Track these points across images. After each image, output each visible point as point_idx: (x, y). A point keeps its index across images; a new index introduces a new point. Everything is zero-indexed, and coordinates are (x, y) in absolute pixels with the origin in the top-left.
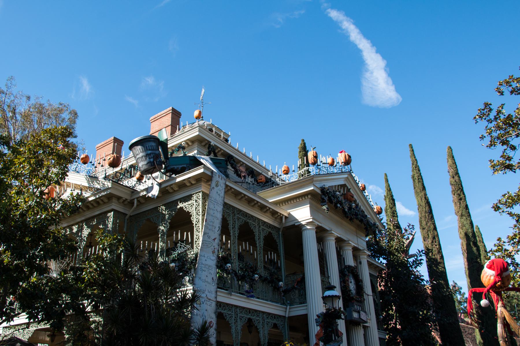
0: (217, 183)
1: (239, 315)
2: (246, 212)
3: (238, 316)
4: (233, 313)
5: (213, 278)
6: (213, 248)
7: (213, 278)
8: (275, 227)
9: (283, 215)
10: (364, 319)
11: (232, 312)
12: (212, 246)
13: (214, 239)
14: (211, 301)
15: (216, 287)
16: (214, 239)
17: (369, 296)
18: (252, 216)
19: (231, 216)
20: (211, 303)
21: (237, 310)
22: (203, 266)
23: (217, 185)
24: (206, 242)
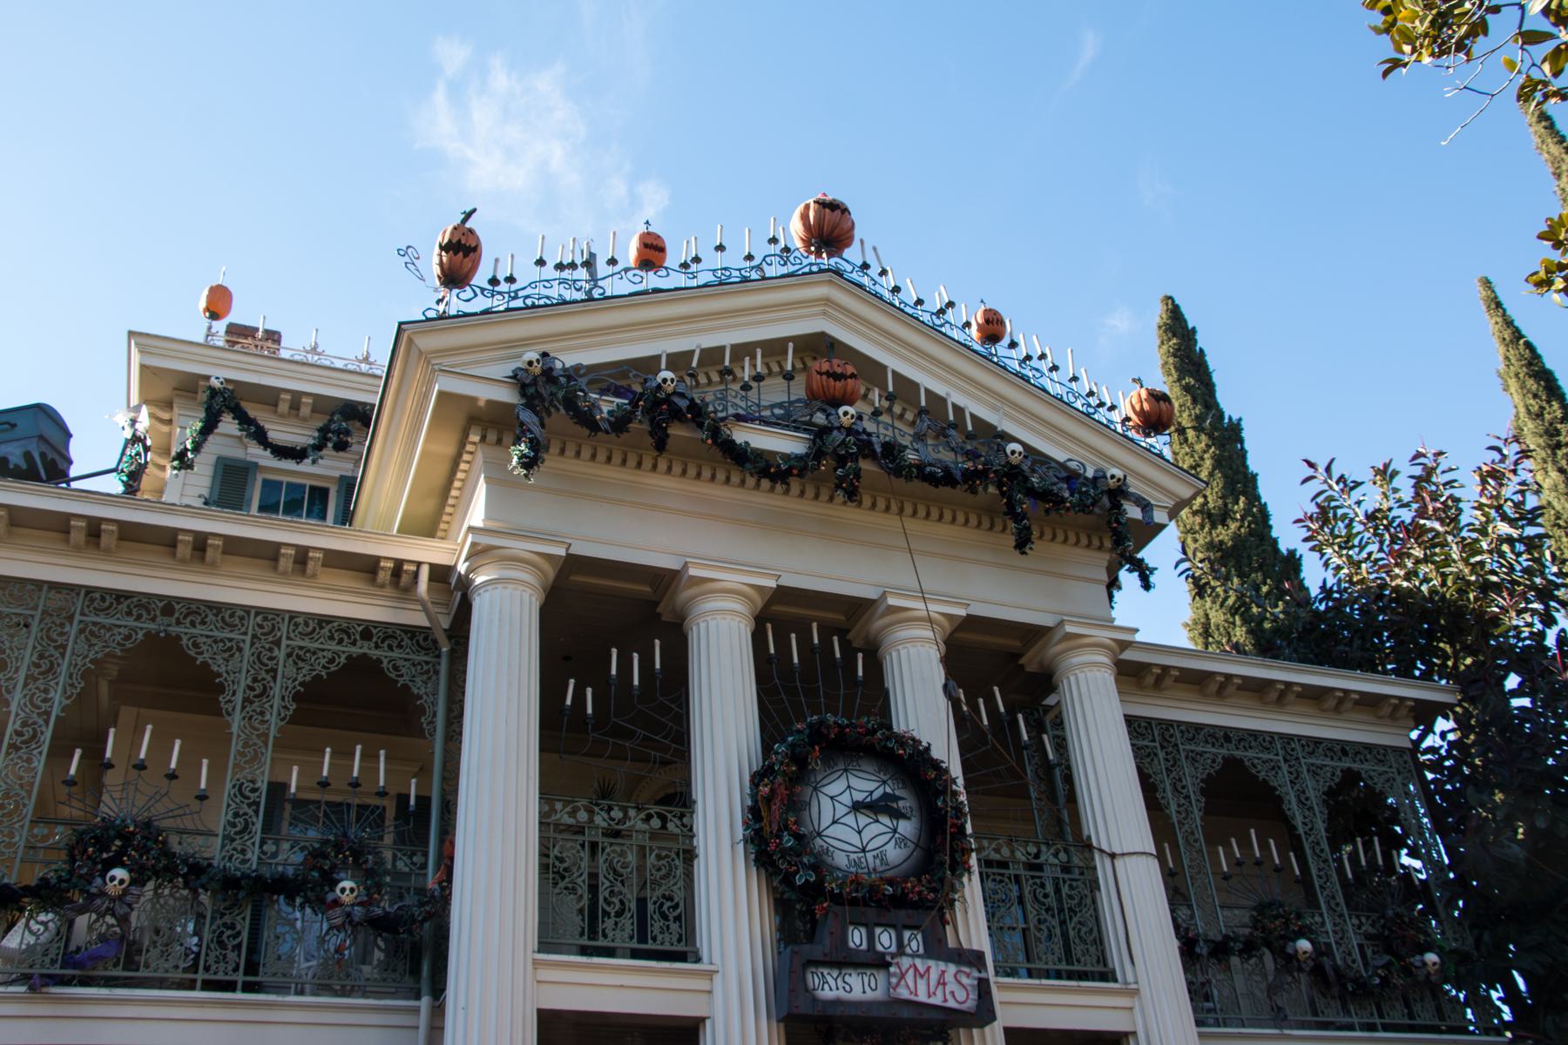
2: (161, 597)
8: (411, 631)
9: (419, 564)
10: (937, 1000)
17: (1119, 863)
18: (216, 608)
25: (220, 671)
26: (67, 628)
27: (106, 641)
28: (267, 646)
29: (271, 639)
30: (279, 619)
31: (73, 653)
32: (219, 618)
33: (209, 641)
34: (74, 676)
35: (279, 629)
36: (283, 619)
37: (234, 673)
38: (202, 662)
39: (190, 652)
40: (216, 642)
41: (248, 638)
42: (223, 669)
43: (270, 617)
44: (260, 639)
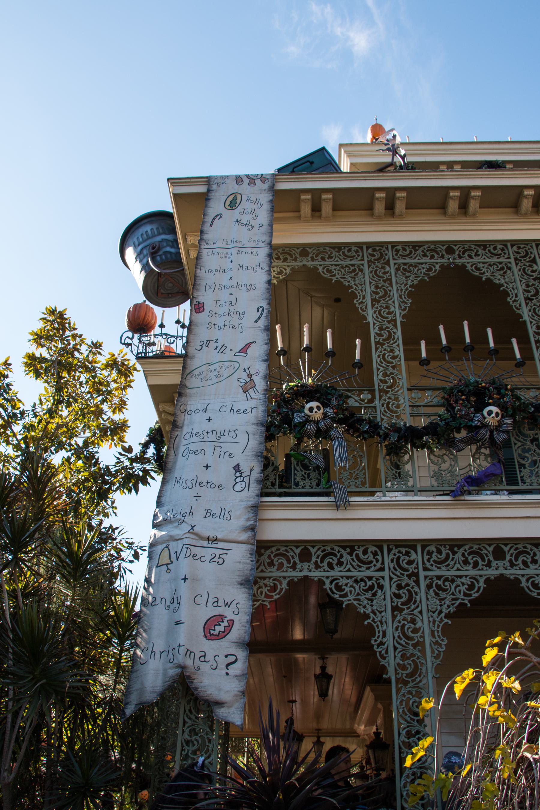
0: (235, 199)
1: (422, 574)
3: (417, 582)
4: (386, 573)
5: (237, 468)
6: (244, 375)
7: (237, 468)
11: (382, 569)
12: (241, 370)
13: (244, 350)
14: (221, 545)
15: (255, 489)
16: (244, 350)
19: (366, 271)
20: (218, 552)
21: (413, 556)
22: (195, 439)
23: (233, 205)
24: (212, 368)
25: (501, 283)
26: (387, 269)
27: (415, 274)
28: (527, 264)
29: (528, 260)
30: (529, 247)
31: (397, 283)
32: (487, 251)
33: (486, 265)
34: (403, 296)
35: (531, 253)
36: (532, 247)
37: (512, 283)
38: (486, 279)
39: (475, 273)
40: (490, 265)
41: (512, 260)
42: (502, 281)
43: (522, 246)
44: (521, 260)
